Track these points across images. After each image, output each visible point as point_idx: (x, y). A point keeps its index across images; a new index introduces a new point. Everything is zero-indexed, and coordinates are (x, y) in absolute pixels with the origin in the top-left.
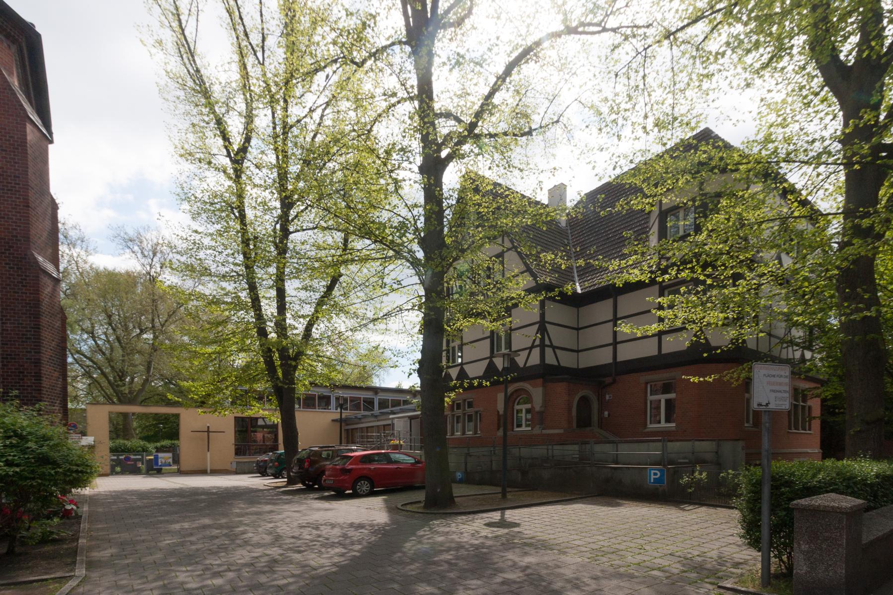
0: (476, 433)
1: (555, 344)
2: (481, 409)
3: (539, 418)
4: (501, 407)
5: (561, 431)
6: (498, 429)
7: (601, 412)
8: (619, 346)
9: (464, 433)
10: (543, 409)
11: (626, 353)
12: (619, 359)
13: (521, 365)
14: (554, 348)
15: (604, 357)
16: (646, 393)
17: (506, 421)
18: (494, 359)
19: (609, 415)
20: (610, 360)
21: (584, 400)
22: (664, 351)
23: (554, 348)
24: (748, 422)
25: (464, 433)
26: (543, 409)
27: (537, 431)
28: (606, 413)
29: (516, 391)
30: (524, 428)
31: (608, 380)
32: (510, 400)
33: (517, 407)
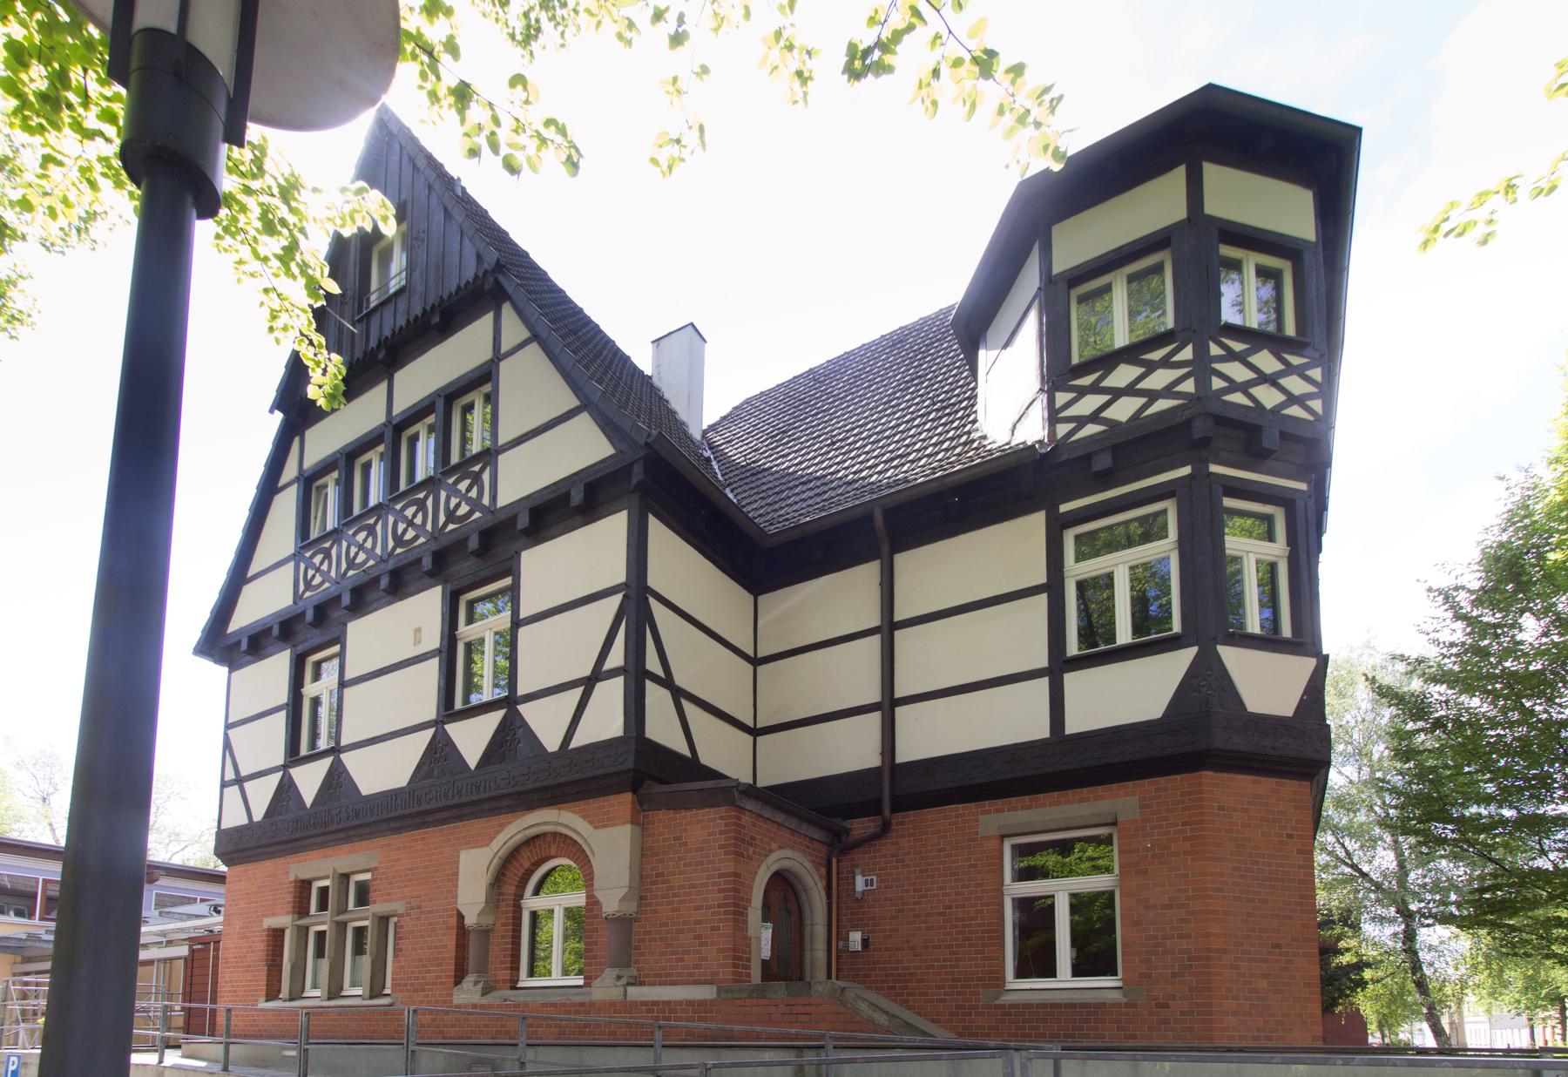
0: (376, 992)
1: (680, 680)
2: (399, 906)
3: (606, 939)
4: (471, 897)
5: (705, 993)
6: (458, 980)
7: (836, 931)
8: (900, 712)
9: (335, 992)
10: (631, 908)
11: (929, 735)
12: (904, 754)
13: (552, 743)
14: (678, 694)
15: (850, 749)
16: (515, 967)
17: (489, 948)
18: (452, 729)
19: (865, 942)
20: (872, 760)
21: (782, 883)
22: (1073, 726)
23: (678, 694)
24: (321, 935)
25: (335, 992)
26: (631, 908)
27: (607, 989)
28: (856, 937)
29: (529, 842)
30: (556, 979)
31: (860, 827)
32: (511, 876)
33: (531, 903)
